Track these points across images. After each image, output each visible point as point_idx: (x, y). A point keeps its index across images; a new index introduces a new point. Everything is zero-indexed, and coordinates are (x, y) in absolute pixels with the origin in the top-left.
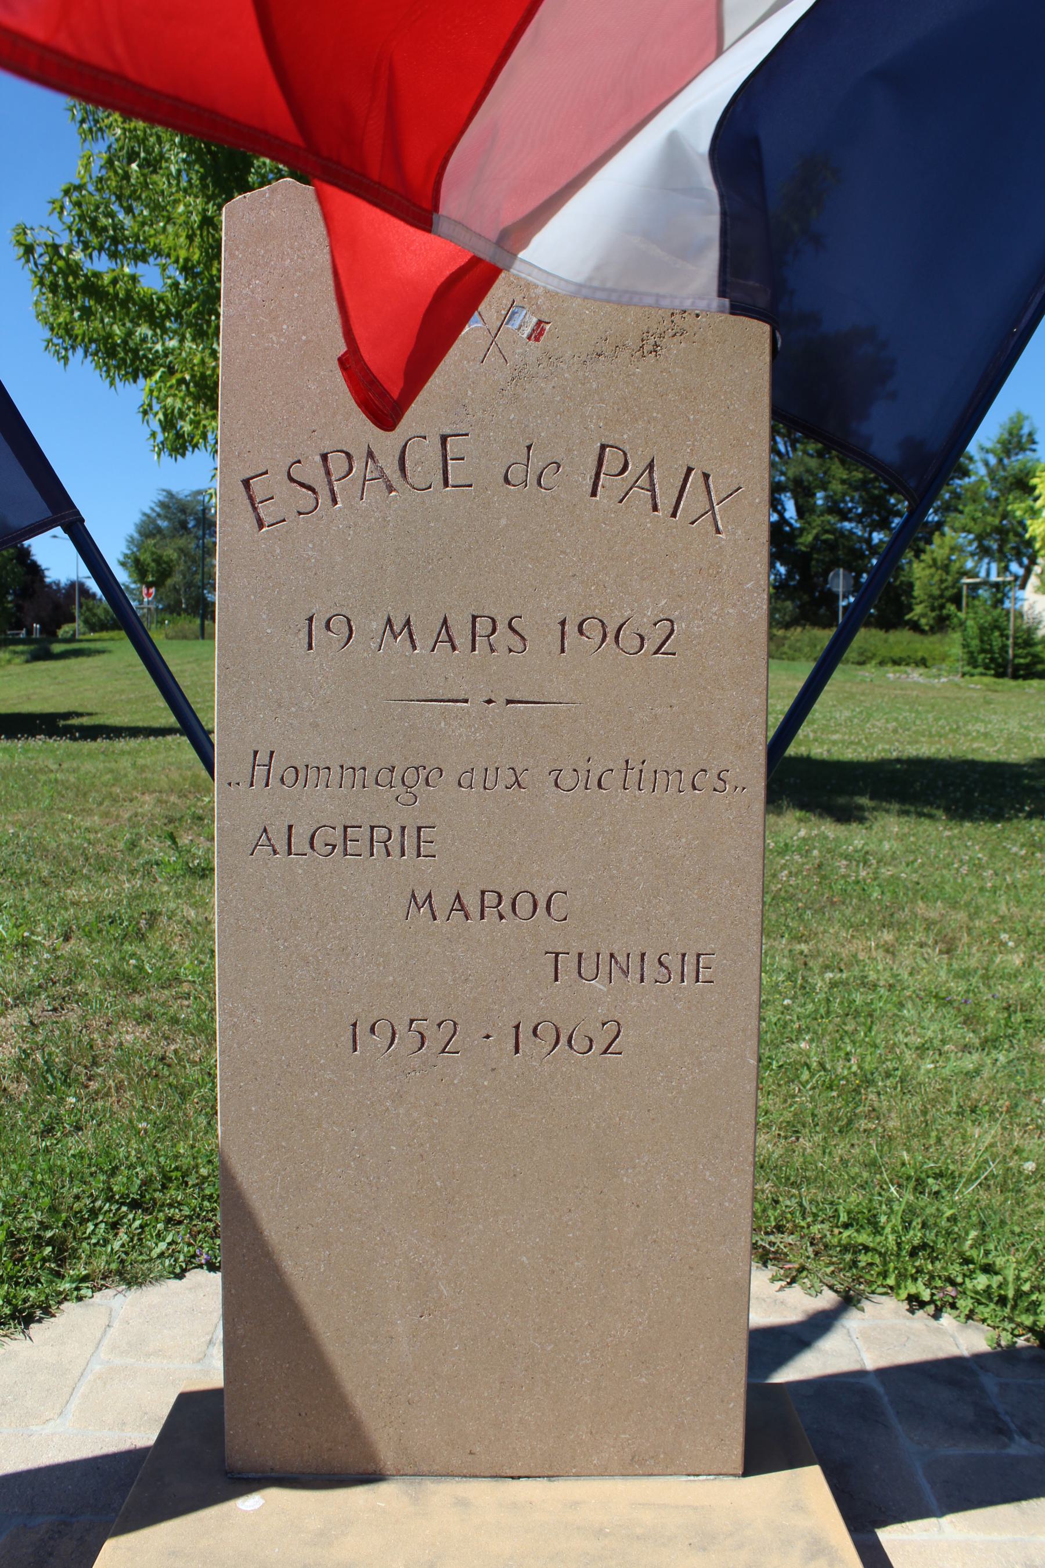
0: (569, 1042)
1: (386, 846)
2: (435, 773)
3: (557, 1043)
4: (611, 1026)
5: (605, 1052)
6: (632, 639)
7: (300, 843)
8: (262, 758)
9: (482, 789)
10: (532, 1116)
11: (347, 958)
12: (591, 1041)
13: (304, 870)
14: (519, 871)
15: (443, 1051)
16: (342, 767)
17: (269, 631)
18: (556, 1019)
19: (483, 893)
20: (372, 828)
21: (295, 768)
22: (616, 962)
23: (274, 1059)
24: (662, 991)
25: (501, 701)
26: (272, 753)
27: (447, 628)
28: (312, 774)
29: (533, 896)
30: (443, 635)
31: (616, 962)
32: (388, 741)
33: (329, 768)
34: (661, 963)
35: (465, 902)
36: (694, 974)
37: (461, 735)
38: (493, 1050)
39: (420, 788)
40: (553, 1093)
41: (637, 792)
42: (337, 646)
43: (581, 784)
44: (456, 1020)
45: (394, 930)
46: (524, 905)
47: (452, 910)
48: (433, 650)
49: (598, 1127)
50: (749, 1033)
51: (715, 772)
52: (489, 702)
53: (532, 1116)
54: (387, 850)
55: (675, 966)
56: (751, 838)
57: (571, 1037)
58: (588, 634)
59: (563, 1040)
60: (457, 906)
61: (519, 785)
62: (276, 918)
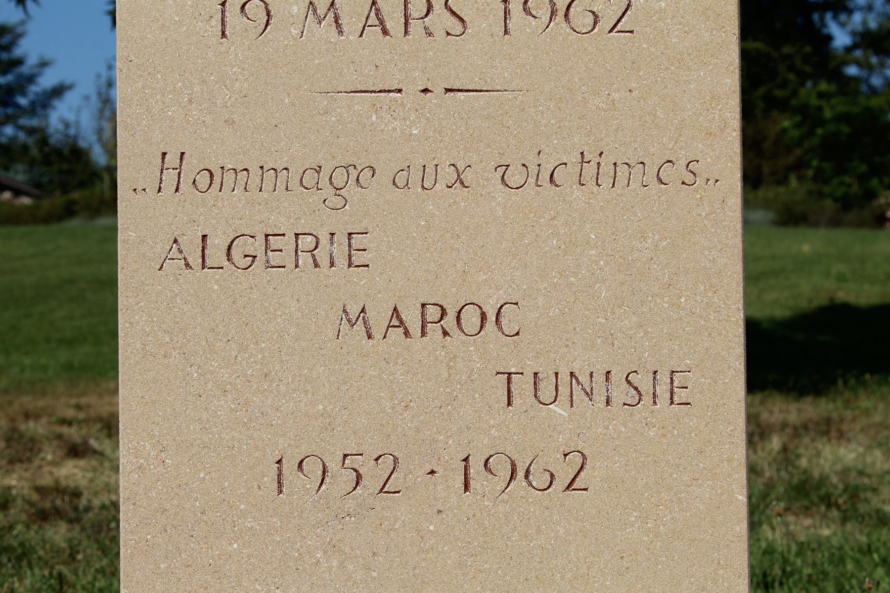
0: (527, 477)
1: (313, 256)
2: (367, 173)
3: (512, 477)
4: (577, 459)
5: (568, 488)
6: (584, 17)
7: (216, 256)
8: (172, 160)
9: (420, 190)
10: (486, 566)
11: (271, 385)
12: (552, 476)
13: (220, 286)
14: (464, 280)
15: (381, 491)
16: (262, 167)
17: (177, 19)
18: (509, 449)
19: (423, 305)
20: (297, 235)
21: (209, 171)
22: (578, 382)
23: (188, 506)
24: (631, 415)
25: (439, 90)
26: (183, 154)
27: (377, 10)
28: (229, 177)
29: (480, 308)
30: (373, 20)
31: (578, 382)
32: (313, 138)
33: (246, 170)
34: (629, 382)
35: (404, 318)
36: (669, 395)
37: (395, 129)
38: (439, 488)
39: (351, 191)
40: (509, 538)
41: (596, 188)
42: (253, 33)
43: (532, 180)
44: (396, 454)
45: (324, 352)
46: (471, 318)
47: (389, 326)
48: (361, 36)
49: (563, 578)
50: (736, 463)
51: (684, 162)
52: (426, 91)
53: (486, 566)
54: (315, 260)
55: (645, 385)
56: (727, 236)
57: (528, 472)
58: (534, 13)
59: (521, 474)
60: (395, 322)
61: (462, 183)
62: (189, 341)
